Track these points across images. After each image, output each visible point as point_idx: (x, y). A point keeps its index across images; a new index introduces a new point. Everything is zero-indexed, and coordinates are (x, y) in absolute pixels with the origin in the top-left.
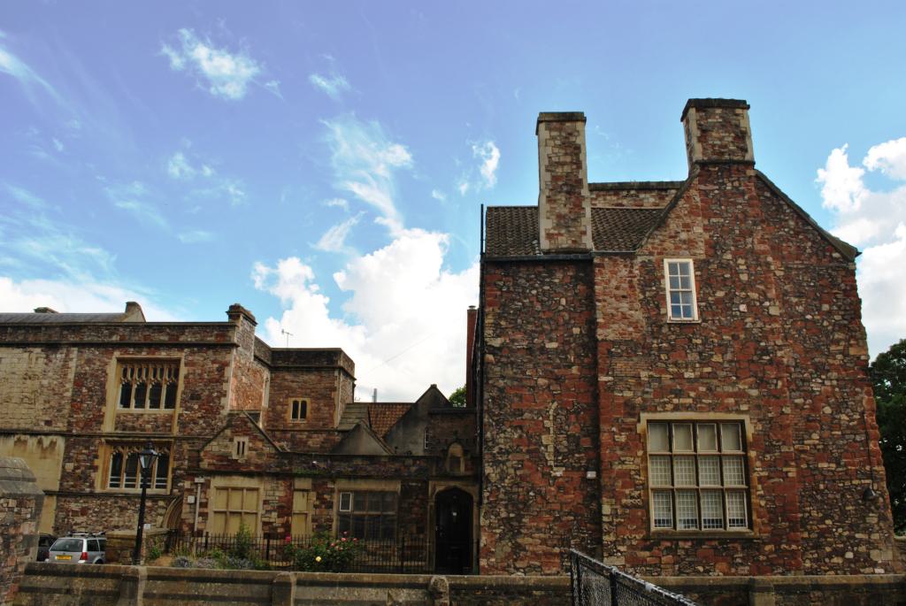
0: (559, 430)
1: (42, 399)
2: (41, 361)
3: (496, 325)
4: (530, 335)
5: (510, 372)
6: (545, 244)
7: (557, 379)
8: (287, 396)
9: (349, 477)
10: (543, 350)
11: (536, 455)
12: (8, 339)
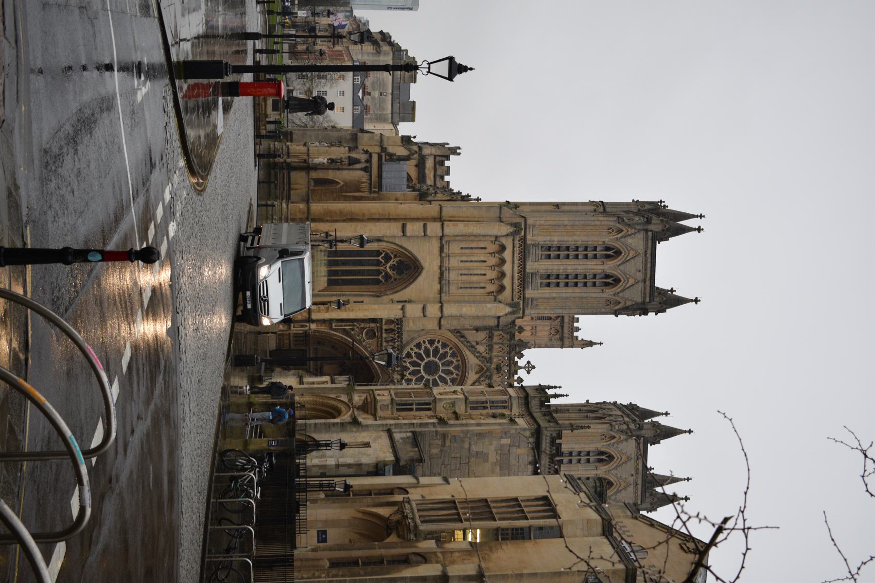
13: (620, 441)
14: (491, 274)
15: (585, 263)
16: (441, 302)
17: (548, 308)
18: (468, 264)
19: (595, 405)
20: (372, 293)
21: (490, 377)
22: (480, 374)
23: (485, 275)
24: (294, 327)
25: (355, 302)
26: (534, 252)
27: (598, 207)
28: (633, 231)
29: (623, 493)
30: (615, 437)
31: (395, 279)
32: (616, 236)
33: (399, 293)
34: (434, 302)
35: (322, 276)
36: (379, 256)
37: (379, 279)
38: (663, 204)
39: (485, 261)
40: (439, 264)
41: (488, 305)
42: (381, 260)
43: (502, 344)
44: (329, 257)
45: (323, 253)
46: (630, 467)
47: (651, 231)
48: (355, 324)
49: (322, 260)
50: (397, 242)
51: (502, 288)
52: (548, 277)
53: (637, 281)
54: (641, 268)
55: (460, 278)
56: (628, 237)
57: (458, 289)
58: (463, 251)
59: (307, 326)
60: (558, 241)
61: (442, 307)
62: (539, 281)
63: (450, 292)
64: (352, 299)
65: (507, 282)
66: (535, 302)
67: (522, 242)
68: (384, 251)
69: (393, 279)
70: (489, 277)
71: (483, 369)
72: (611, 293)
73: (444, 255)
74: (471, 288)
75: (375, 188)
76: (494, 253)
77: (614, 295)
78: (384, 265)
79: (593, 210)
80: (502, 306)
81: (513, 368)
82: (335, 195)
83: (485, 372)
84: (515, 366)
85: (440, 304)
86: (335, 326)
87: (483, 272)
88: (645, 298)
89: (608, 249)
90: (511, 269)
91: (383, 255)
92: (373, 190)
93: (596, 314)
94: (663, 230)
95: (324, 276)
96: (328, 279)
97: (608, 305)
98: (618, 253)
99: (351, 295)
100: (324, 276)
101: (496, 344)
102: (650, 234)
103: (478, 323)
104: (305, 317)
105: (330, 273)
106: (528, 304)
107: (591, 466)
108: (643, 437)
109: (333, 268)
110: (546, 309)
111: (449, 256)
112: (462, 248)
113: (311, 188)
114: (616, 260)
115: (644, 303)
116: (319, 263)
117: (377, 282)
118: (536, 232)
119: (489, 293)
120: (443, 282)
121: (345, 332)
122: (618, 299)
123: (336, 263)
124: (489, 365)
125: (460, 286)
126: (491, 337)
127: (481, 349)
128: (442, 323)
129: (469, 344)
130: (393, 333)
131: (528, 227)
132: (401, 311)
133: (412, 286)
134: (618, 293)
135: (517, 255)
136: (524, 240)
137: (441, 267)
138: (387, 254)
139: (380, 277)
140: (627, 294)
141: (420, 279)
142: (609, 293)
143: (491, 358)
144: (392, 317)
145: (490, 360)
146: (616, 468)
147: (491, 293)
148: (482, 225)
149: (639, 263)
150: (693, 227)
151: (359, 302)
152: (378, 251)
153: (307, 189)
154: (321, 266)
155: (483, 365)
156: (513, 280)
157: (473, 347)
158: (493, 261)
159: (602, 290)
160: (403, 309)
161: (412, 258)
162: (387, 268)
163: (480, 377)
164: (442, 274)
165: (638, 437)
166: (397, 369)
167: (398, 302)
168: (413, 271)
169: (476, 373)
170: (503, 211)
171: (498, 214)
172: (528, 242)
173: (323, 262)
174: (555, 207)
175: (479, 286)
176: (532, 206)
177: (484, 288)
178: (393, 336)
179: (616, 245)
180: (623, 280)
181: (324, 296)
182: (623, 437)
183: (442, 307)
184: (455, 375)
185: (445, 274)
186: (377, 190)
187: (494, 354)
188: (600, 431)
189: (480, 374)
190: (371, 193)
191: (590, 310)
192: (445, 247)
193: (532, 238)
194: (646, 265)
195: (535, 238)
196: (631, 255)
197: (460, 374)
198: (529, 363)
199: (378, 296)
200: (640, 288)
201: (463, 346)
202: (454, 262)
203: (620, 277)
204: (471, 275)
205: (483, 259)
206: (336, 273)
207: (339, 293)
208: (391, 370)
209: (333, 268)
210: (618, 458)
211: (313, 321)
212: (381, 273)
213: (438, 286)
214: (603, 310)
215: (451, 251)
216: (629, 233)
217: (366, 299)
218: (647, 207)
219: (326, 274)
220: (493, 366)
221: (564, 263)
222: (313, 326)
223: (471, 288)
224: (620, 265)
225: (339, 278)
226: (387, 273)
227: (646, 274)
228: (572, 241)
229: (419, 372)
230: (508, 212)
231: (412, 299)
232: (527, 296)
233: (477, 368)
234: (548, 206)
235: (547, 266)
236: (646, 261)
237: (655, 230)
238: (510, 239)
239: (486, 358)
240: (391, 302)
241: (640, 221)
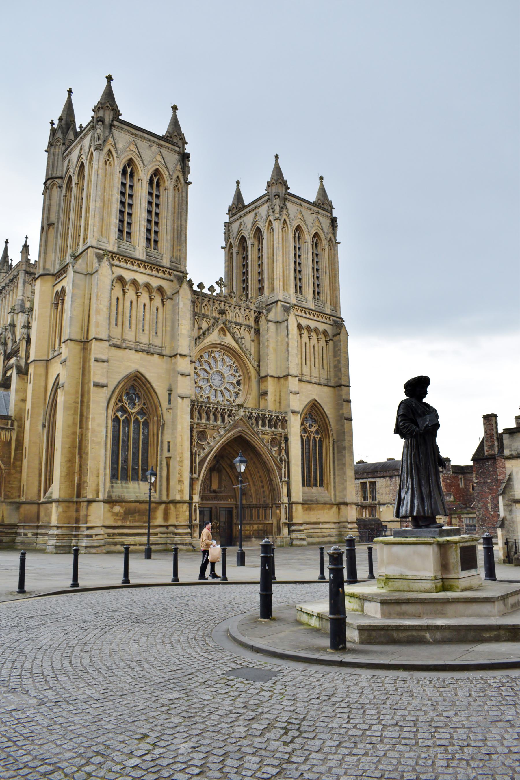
0: (492, 502)
1: (391, 493)
2: (389, 481)
3: (476, 477)
4: (484, 478)
5: (480, 488)
6: (486, 454)
7: (491, 489)
8: (470, 483)
9: (467, 514)
10: (487, 482)
11: (487, 510)
12: (379, 475)
13: (288, 215)
14: (145, 297)
15: (140, 198)
16: (175, 356)
17: (179, 248)
18: (134, 321)
19: (231, 240)
20: (160, 431)
21: (231, 322)
22: (227, 331)
23: (145, 305)
24: (195, 520)
25: (169, 450)
26: (125, 247)
27: (54, 184)
28: (111, 139)
29: (324, 226)
30: (285, 220)
31: (144, 404)
32: (115, 159)
33: (161, 401)
34: (175, 363)
35: (139, 488)
36: (119, 420)
37: (143, 422)
38: (56, 122)
39: (131, 302)
40: (134, 352)
41: (181, 305)
42: (123, 418)
43: (202, 304)
44: (117, 479)
45: (114, 485)
46: (306, 213)
47: (112, 121)
48: (194, 451)
49: (122, 486)
51: (160, 290)
52: (148, 240)
53: (159, 153)
54: (148, 145)
55: (146, 332)
56: (117, 146)
57: (158, 336)
58: (120, 323)
59: (195, 506)
60: (116, 218)
61: (181, 355)
62: (153, 250)
63: (160, 345)
64: (166, 454)
65: (155, 283)
66: (173, 260)
67: (115, 257)
68: (115, 414)
69: (145, 407)
70: (147, 302)
71: (222, 328)
72: (169, 182)
73: (124, 345)
74: (157, 322)
75: (7, 424)
76: (123, 290)
77: (171, 179)
78: (129, 415)
79: (59, 189)
80: (181, 291)
81: (223, 299)
82: (13, 471)
83: (225, 326)
84: (220, 296)
85: (178, 356)
86: (195, 473)
87: (142, 307)
88: (175, 151)
89: (124, 173)
90: (142, 275)
92: (9, 427)
93: (187, 202)
94: (112, 110)
95: (139, 484)
96: (142, 480)
97: (178, 189)
98: (130, 162)
99: (161, 455)
100: (139, 484)
101: (201, 310)
102: (115, 123)
103: (192, 322)
105: (135, 478)
106: (176, 267)
107: (303, 246)
108: (285, 195)
109: (130, 473)
110: (180, 250)
111: (124, 340)
112: (116, 325)
113: (3, 499)
114: (138, 166)
115: (179, 153)
116: (125, 490)
117: (146, 424)
118: (104, 240)
119: (163, 305)
120: (152, 350)
122: (174, 177)
123: (125, 470)
124: (220, 321)
125: (155, 334)
127: (205, 326)
129: (202, 337)
130: (201, 411)
131: (99, 247)
132: (184, 399)
133: (154, 385)
134: (170, 174)
135: (129, 266)
136: (112, 255)
137: (137, 351)
138: (118, 411)
139: (142, 421)
140: (171, 166)
141: (147, 375)
142: (168, 183)
143: (214, 318)
144: (189, 409)
145: (216, 320)
146: (307, 226)
147: (163, 302)
148: (99, 294)
149: (143, 145)
150: (106, 83)
151: (169, 446)
152: (114, 419)
153: (4, 504)
154: (128, 488)
155: (220, 327)
156: (153, 276)
157: (204, 334)
158: (131, 293)
159: (165, 189)
160: (182, 398)
161: (126, 381)
162: (133, 411)
163: (230, 333)
164: (143, 351)
165: (285, 199)
166: (234, 411)
167: (170, 404)
168: (138, 382)
169: (225, 335)
170: (79, 270)
171: (83, 276)
172: (115, 250)
173: (124, 485)
174: (51, 228)
175: (155, 313)
176: (48, 252)
177: (157, 309)
178: (204, 412)
179: (124, 161)
180: (158, 167)
181: (161, 485)
182: (285, 211)
183: (181, 355)
184: (224, 357)
185: (143, 348)
186: (10, 422)
187: (209, 314)
188: (280, 230)
189: (227, 331)
190: (14, 429)
191: (184, 207)
192: (115, 343)
193: (111, 245)
194: (145, 139)
195: (112, 242)
196: (134, 150)
197: (223, 352)
198: (217, 283)
199: (163, 425)
200: (166, 152)
201: (202, 343)
202: (130, 335)
203: (154, 168)
204: (144, 320)
205: (128, 304)
206: (135, 471)
207: (158, 468)
208: (235, 417)
209: (130, 473)
211: (191, 498)
212: (137, 419)
213: (156, 356)
214: (184, 194)
215: (119, 337)
216: (113, 144)
217: (167, 437)
218: (59, 135)
219: (136, 482)
220: (220, 316)
221: (138, 219)
222: (196, 498)
223: (157, 322)
224: (144, 164)
225: (140, 468)
226: (138, 413)
227: (154, 142)
228: (117, 205)
229: (221, 391)
230: (81, 265)
231: (167, 387)
232: (168, 265)
233: (221, 334)
234: (49, 235)
235: (141, 237)
236: (141, 137)
237: (111, 117)
238: (114, 268)
239: (214, 323)
240: (170, 411)
241: (102, 128)
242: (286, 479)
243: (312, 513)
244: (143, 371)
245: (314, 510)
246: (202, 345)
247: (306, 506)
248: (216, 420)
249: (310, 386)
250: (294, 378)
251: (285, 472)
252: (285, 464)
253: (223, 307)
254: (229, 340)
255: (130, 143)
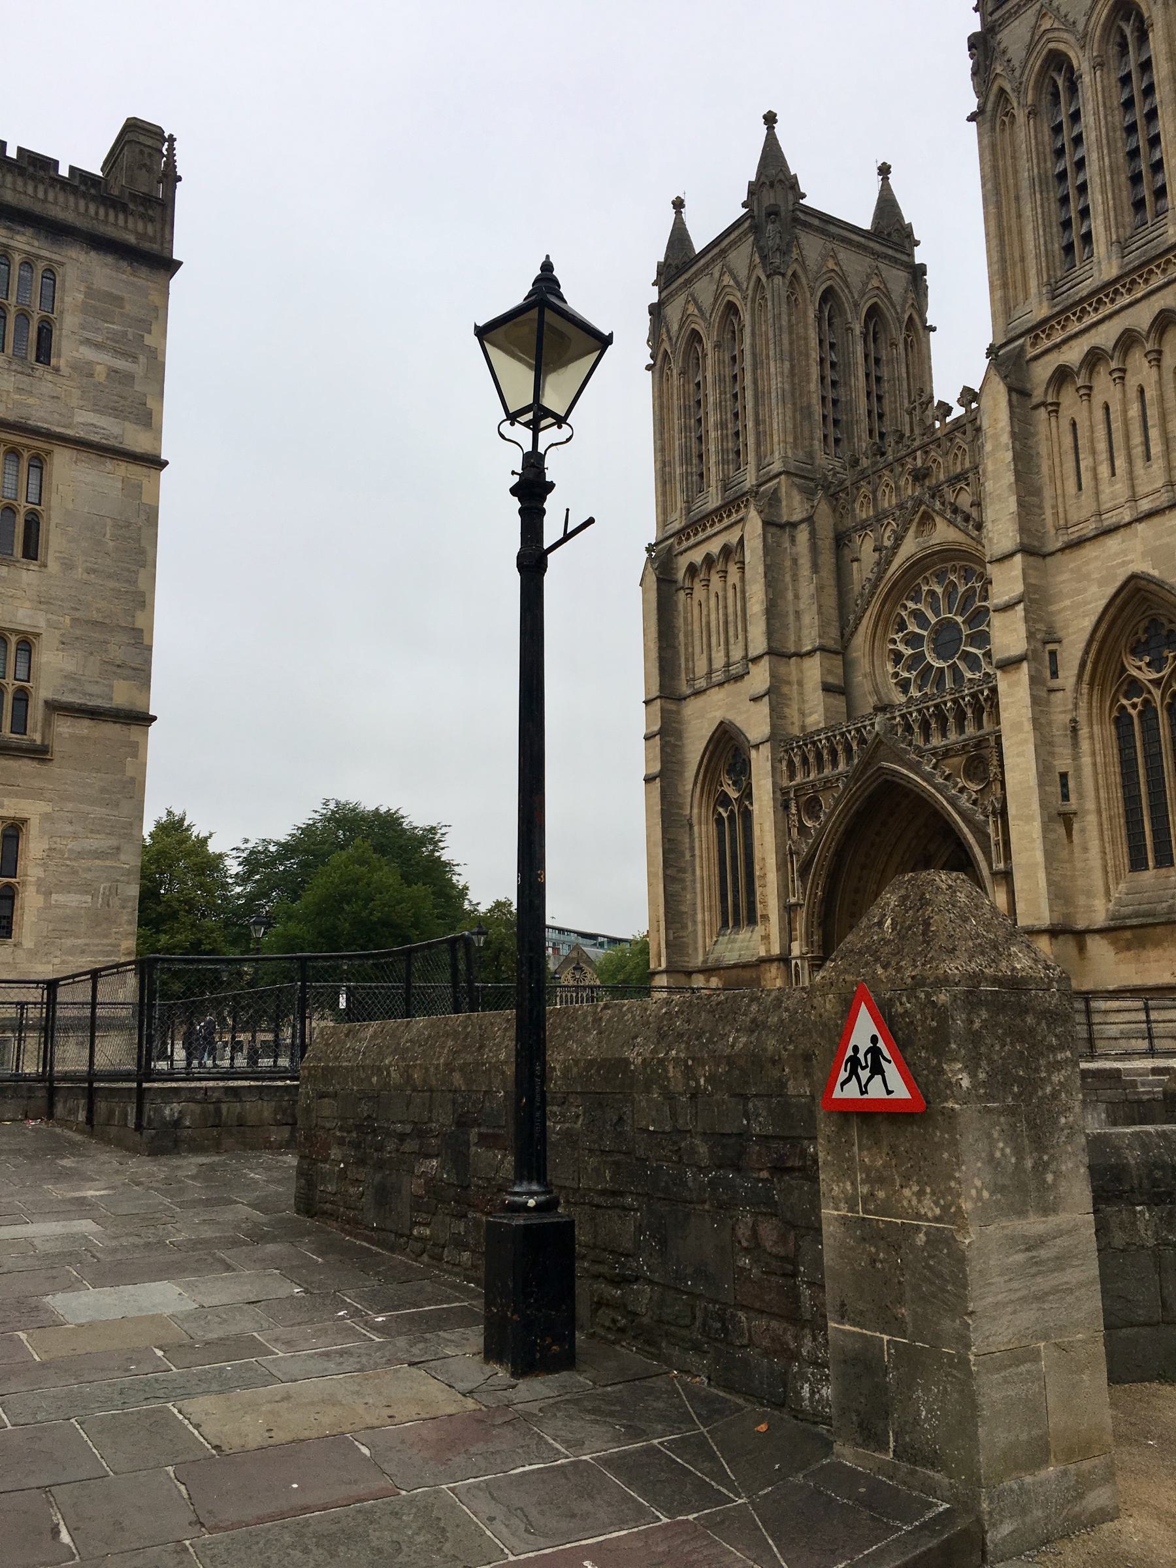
50: (691, 786)
91: (721, 810)
104: (778, 968)
121: (804, 872)
126: (864, 526)
128: (809, 648)
137: (721, 684)
140: (742, 274)
160: (757, 747)
161: (711, 747)
209: (743, 912)
210: (1049, 41)
222: (796, 949)
227: (713, 260)
242: (1002, 866)
243: (1153, 954)
244: (731, 716)
245: (1157, 944)
246: (883, 588)
247: (1128, 934)
248: (835, 764)
249: (1113, 543)
250: (1007, 564)
251: (997, 844)
252: (995, 822)
253: (919, 462)
254: (944, 533)
255: (687, 302)
